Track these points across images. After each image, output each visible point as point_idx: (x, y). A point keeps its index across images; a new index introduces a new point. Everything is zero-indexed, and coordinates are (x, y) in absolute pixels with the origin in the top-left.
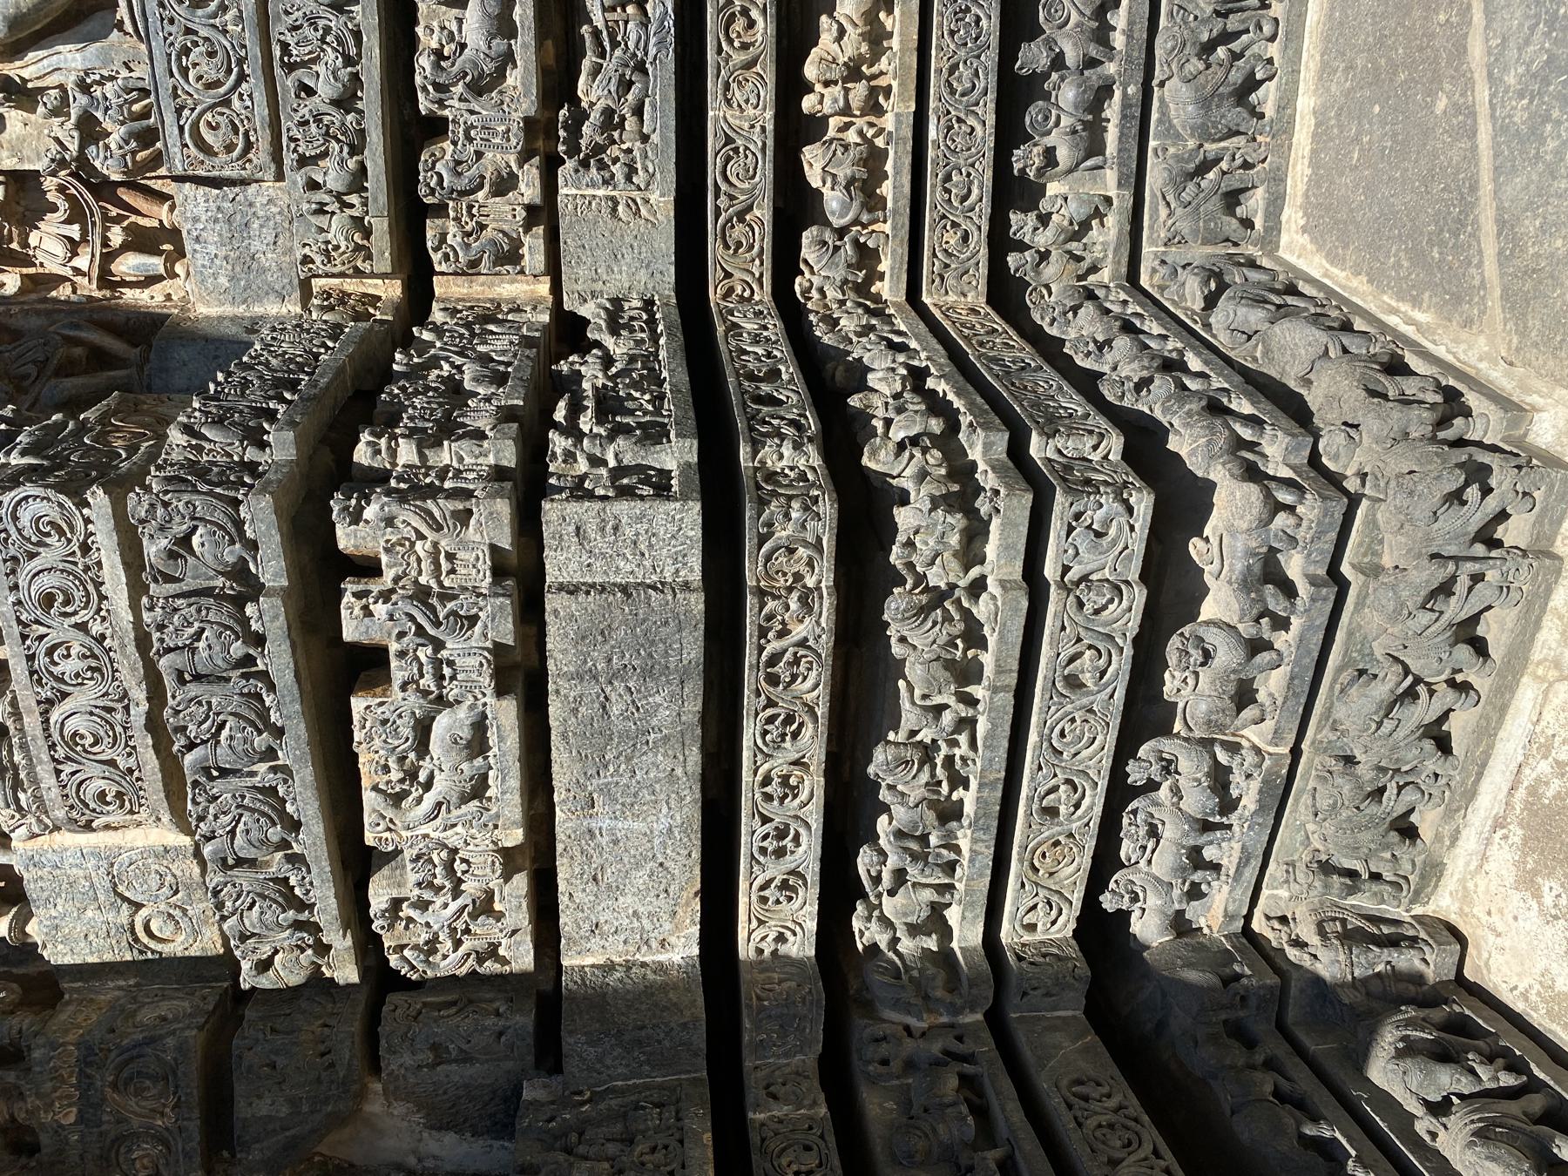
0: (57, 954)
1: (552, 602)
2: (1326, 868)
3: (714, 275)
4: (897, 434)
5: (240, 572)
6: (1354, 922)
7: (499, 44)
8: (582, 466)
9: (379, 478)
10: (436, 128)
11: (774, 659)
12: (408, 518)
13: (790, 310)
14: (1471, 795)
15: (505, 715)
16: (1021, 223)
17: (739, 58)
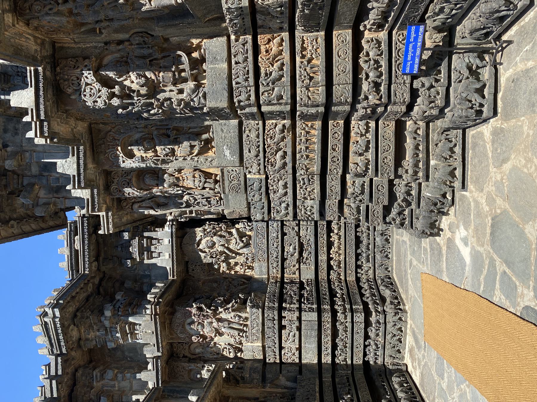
0: (245, 358)
1: (302, 322)
2: (391, 356)
3: (320, 276)
4: (339, 304)
5: (273, 318)
6: (395, 363)
7: (294, 251)
8: (305, 307)
9: (285, 309)
10: (287, 259)
11: (325, 329)
12: (289, 313)
13: (329, 281)
14: (405, 348)
15: (297, 333)
16: (359, 270)
17: (322, 252)
